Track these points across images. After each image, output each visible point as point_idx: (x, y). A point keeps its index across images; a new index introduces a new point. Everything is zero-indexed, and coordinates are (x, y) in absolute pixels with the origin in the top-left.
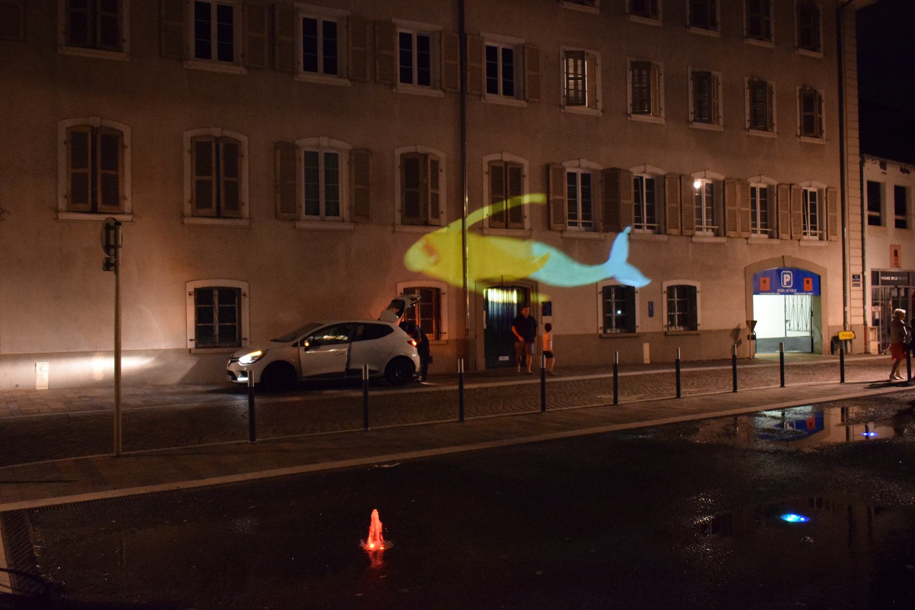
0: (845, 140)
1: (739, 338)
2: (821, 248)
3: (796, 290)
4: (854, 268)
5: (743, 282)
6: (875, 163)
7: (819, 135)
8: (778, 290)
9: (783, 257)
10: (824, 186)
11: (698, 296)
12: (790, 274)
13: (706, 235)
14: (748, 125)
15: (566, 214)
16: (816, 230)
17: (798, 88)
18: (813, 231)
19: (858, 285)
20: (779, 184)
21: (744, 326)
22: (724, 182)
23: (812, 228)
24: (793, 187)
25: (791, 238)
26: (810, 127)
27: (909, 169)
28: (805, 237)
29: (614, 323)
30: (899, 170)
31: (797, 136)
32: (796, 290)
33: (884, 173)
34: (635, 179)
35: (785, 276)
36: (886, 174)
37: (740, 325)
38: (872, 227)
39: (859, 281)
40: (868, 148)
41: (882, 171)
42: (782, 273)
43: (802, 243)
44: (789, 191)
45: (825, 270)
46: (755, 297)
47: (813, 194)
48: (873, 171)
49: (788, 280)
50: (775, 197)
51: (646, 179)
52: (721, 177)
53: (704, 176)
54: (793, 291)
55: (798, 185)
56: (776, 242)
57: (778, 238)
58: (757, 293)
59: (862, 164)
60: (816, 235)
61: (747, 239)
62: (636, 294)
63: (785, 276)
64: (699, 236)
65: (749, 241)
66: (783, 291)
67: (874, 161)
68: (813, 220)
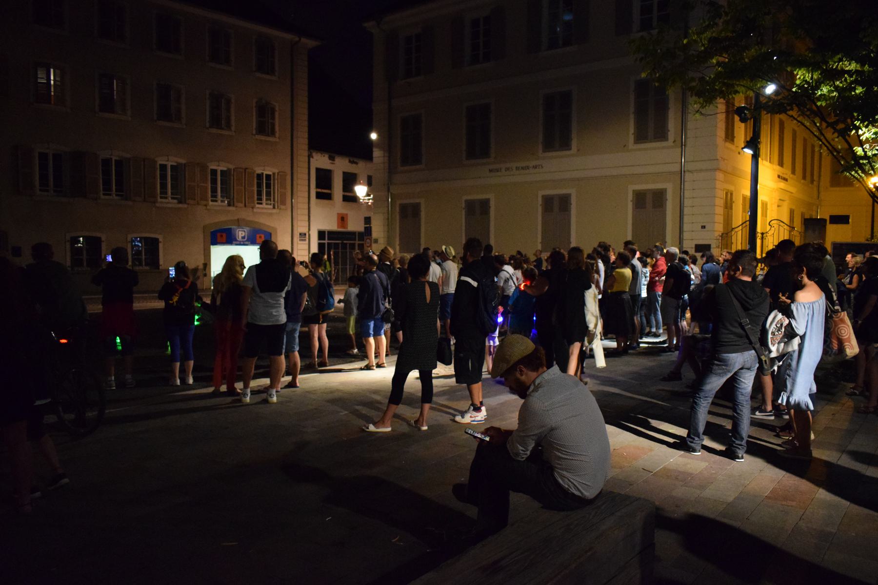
0: (295, 140)
1: (196, 276)
2: (271, 214)
3: (249, 243)
4: (301, 228)
5: (201, 236)
6: (324, 156)
7: (273, 133)
8: (234, 242)
9: (238, 219)
10: (276, 171)
11: (161, 245)
12: (245, 231)
13: (170, 203)
14: (208, 125)
15: (37, 183)
16: (271, 201)
17: (255, 100)
18: (269, 202)
19: (305, 240)
20: (236, 168)
21: (201, 267)
22: (185, 164)
23: (267, 200)
24: (247, 170)
25: (245, 206)
26: (265, 127)
27: (358, 161)
28: (258, 206)
29: (85, 264)
30: (347, 161)
31: (252, 134)
32: (249, 243)
33: (332, 163)
34: (102, 159)
35: (240, 233)
36: (334, 164)
37: (198, 266)
38: (319, 200)
39: (305, 237)
40: (316, 145)
41: (331, 161)
42: (237, 231)
43: (255, 210)
44: (244, 174)
45: (275, 230)
46: (212, 247)
47: (268, 176)
48: (321, 161)
49: (243, 235)
50: (232, 178)
51: (115, 160)
52: (183, 161)
53: (167, 159)
54: (247, 243)
55: (252, 169)
56: (231, 208)
57: (234, 206)
58: (215, 243)
59: (310, 156)
60: (271, 204)
61: (206, 205)
62: (102, 243)
63: (243, 233)
64: (161, 203)
65: (208, 207)
66: (238, 243)
67: (322, 155)
68: (268, 194)
